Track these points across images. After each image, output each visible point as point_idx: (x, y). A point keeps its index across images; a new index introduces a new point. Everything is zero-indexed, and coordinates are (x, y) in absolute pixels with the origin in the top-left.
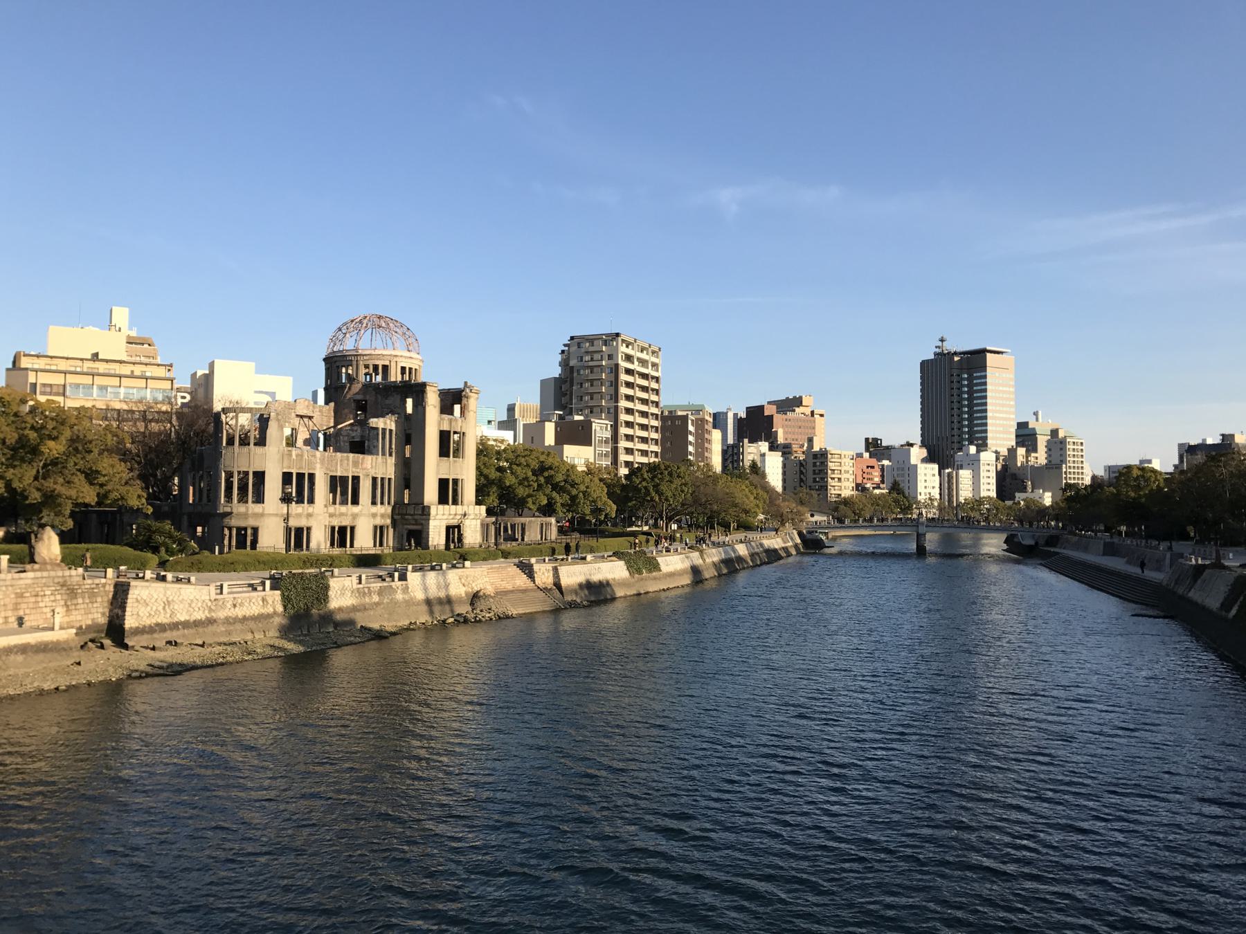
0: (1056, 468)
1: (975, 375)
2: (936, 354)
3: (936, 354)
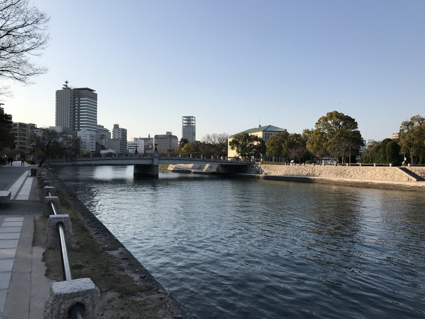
0: (117, 140)
1: (81, 99)
2: (63, 88)
3: (63, 88)
